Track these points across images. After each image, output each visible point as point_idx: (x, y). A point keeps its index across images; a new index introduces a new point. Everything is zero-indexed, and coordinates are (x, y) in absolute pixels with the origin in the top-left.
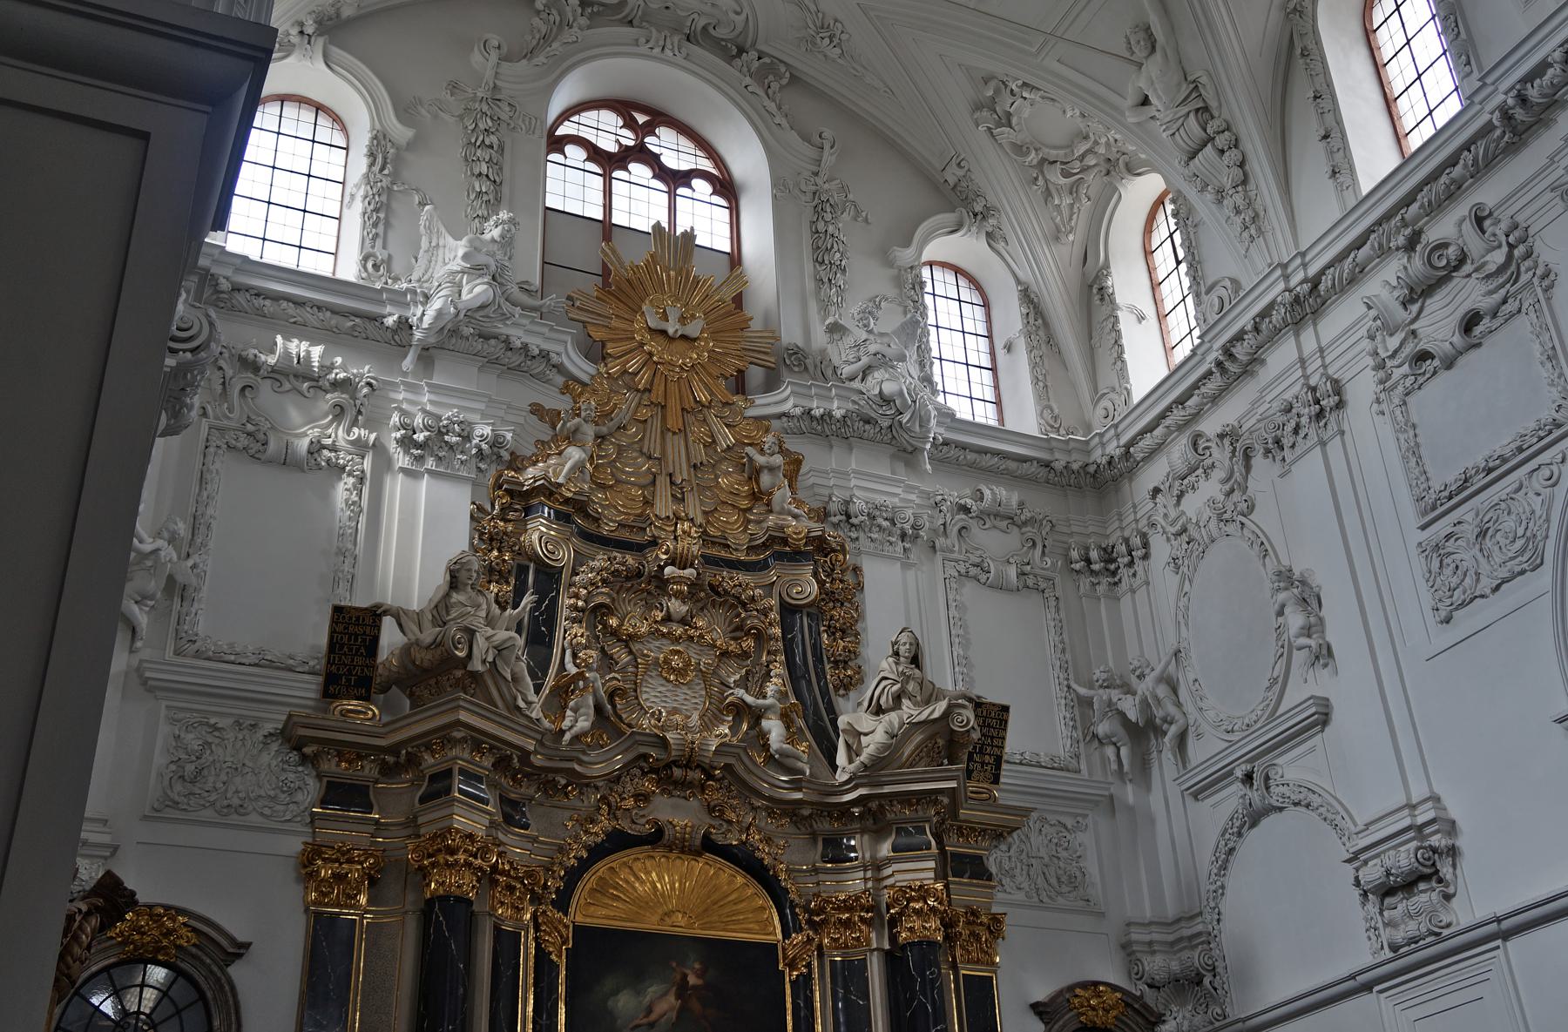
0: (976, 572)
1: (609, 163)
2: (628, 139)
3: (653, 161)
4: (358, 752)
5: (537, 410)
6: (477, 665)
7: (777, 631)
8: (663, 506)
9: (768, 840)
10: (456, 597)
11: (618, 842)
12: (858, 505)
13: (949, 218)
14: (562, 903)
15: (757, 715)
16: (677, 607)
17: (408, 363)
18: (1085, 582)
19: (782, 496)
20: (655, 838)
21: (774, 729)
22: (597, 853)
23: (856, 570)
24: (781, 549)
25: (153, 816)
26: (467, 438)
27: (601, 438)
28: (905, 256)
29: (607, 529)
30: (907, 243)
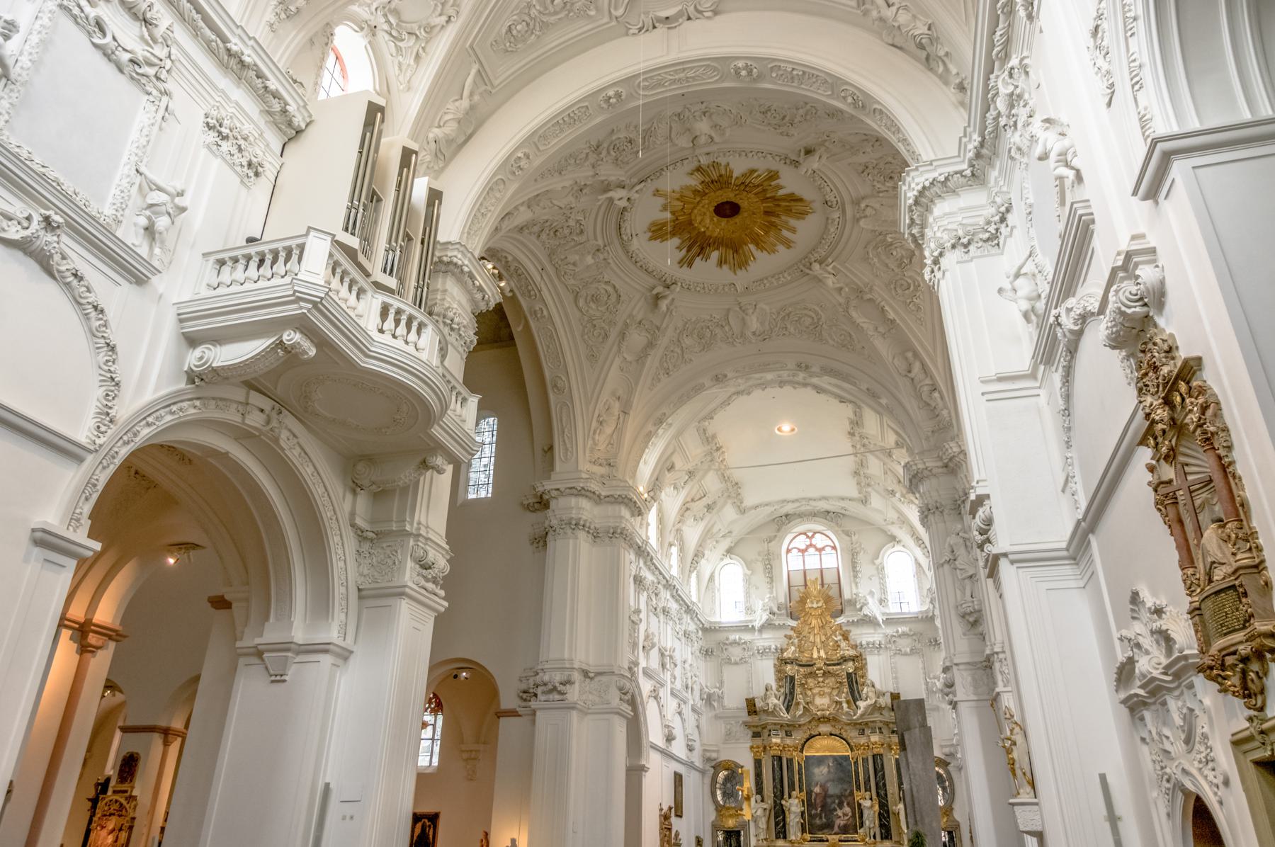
0: (899, 652)
1: (803, 551)
2: (808, 542)
3: (815, 546)
4: (757, 726)
5: (786, 636)
6: (770, 710)
7: (846, 680)
8: (815, 655)
9: (846, 731)
10: (768, 693)
11: (812, 737)
12: (864, 643)
13: (892, 544)
14: (802, 751)
15: (841, 703)
16: (821, 679)
17: (756, 633)
18: (932, 647)
19: (843, 644)
20: (820, 734)
21: (845, 705)
22: (808, 740)
23: (865, 659)
24: (845, 660)
25: (724, 743)
26: (770, 649)
27: (800, 641)
28: (877, 562)
29: (804, 663)
30: (877, 558)
